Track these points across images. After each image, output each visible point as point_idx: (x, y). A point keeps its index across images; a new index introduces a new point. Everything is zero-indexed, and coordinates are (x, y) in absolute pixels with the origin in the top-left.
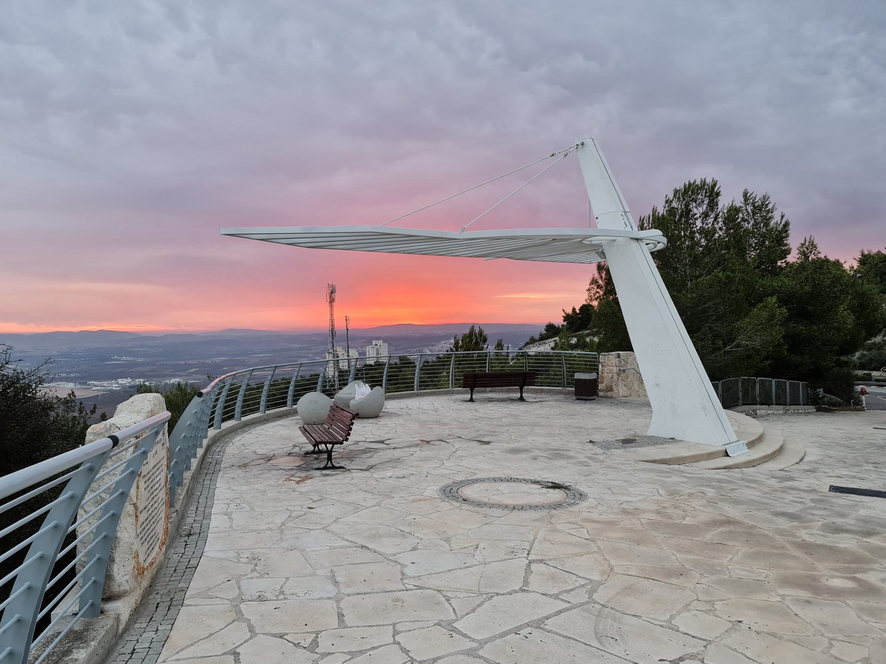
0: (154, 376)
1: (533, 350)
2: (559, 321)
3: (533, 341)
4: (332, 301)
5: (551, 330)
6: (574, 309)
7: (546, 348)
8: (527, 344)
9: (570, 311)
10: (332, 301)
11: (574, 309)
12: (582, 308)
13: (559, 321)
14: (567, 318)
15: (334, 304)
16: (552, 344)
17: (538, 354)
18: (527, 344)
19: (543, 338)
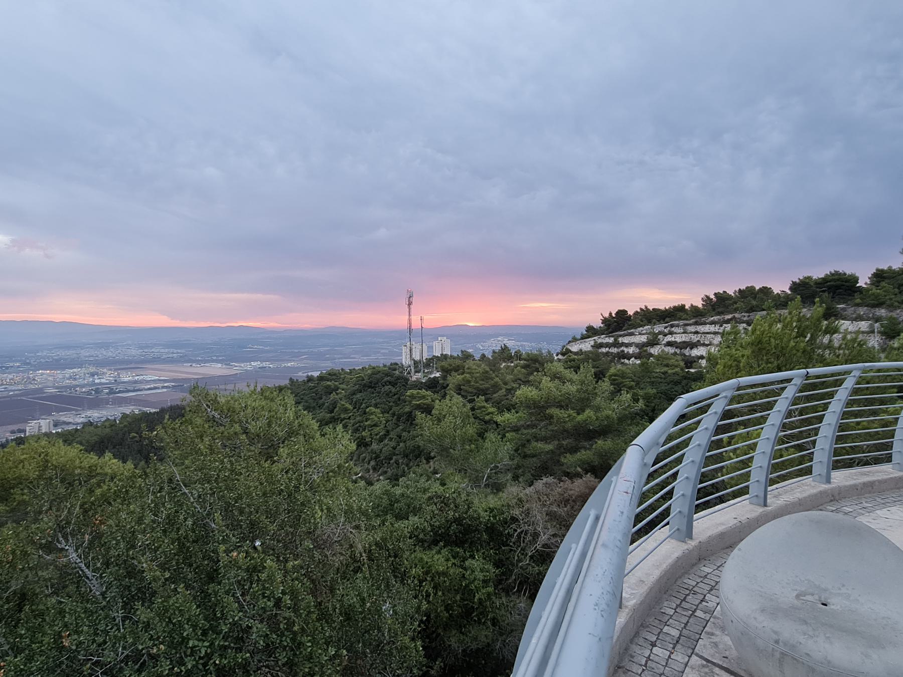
0: (277, 361)
1: (574, 348)
2: (597, 323)
3: (575, 340)
4: (410, 304)
5: (591, 331)
6: (611, 314)
7: (587, 346)
8: (570, 342)
9: (607, 315)
10: (410, 304)
11: (611, 314)
12: (617, 313)
13: (597, 323)
14: (605, 321)
15: (412, 306)
16: (592, 343)
17: (580, 352)
18: (570, 342)
19: (583, 337)
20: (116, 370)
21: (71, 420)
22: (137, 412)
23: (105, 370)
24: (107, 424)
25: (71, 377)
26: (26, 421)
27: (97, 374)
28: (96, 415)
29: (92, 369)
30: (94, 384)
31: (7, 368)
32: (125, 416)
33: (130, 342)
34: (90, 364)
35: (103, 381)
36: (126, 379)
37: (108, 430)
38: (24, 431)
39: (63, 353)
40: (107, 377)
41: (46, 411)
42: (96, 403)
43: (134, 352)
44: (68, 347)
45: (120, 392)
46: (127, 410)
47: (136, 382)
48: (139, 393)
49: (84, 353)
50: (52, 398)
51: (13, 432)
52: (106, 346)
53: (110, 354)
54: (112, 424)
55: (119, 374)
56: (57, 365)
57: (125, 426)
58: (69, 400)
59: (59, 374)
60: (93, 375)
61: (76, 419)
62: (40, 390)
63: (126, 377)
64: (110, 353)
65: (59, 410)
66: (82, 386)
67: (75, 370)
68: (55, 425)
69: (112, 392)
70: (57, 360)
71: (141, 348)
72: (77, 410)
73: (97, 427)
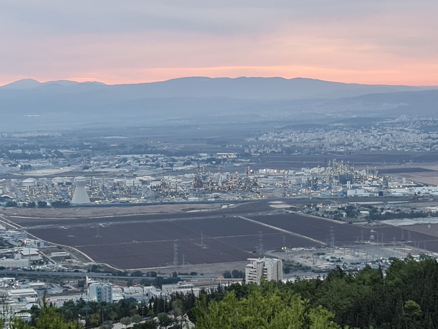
20: (381, 172)
21: (309, 263)
22: (417, 258)
23: (363, 173)
24: (367, 276)
25: (308, 185)
26: (244, 258)
27: (351, 179)
28: (349, 257)
29: (343, 170)
30: (344, 198)
31: (219, 162)
32: (396, 265)
33: (404, 118)
34: (338, 160)
35: (360, 193)
36: (398, 192)
37: (367, 289)
38: (241, 275)
39: (297, 138)
40: (366, 187)
41: (274, 244)
42: (348, 236)
43: (413, 138)
44: (304, 127)
45: (388, 216)
46: (401, 253)
47: (415, 198)
48: (421, 221)
49: (331, 138)
50: (280, 219)
51: (227, 275)
52: (363, 124)
53: (371, 141)
54: (372, 276)
55: (386, 181)
56: (288, 158)
57: (397, 285)
58: (306, 226)
59: (291, 176)
60: (343, 180)
61: (319, 261)
62: (264, 205)
63: (398, 188)
64: (370, 140)
65: (293, 243)
66: (326, 201)
67: (316, 170)
68: (287, 271)
69: (374, 215)
70: (289, 151)
71: (426, 129)
72: (318, 246)
73: (350, 280)
